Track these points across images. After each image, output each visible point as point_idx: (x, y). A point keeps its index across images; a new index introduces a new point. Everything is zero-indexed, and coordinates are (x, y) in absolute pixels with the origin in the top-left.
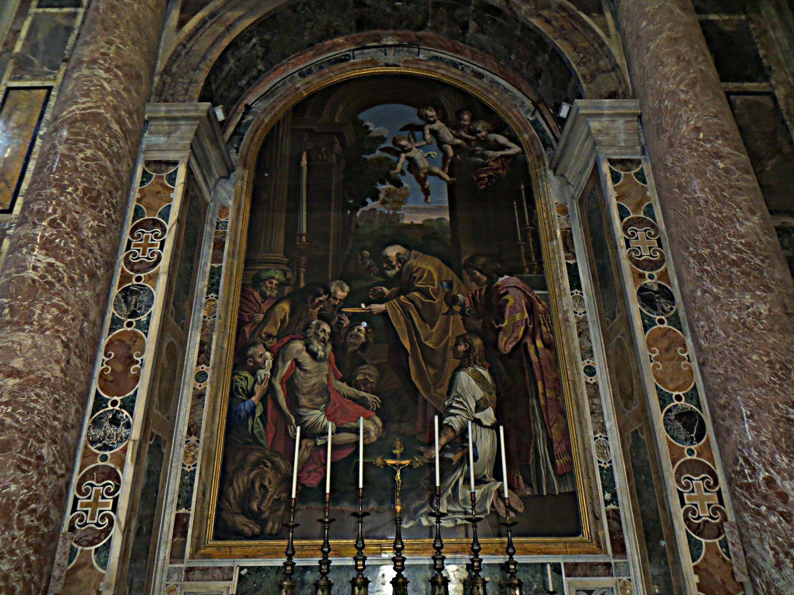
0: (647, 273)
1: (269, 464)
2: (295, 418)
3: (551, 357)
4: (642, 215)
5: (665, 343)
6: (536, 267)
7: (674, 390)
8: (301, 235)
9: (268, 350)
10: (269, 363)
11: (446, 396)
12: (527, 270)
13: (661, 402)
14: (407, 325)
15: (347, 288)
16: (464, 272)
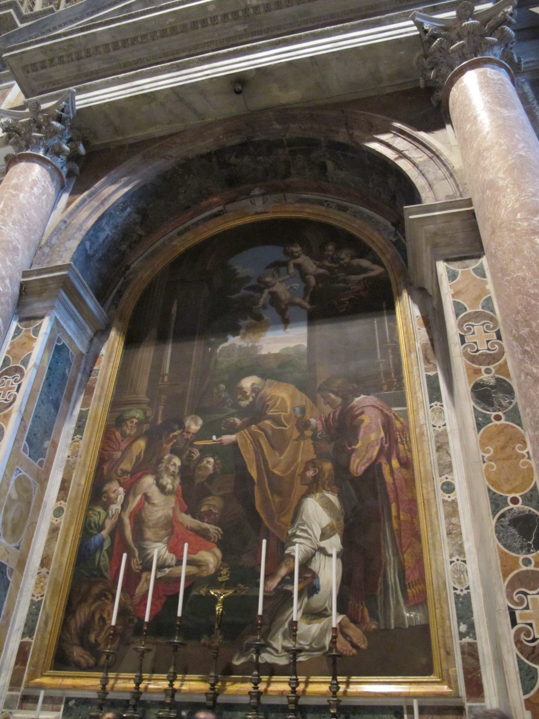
0: (483, 368)
2: (139, 551)
3: (407, 477)
4: (480, 309)
5: (502, 440)
6: (395, 383)
7: (509, 492)
8: (163, 376)
9: (121, 485)
10: (121, 498)
11: (290, 524)
12: (385, 387)
13: (494, 506)
14: (256, 453)
15: (200, 422)
16: (319, 396)
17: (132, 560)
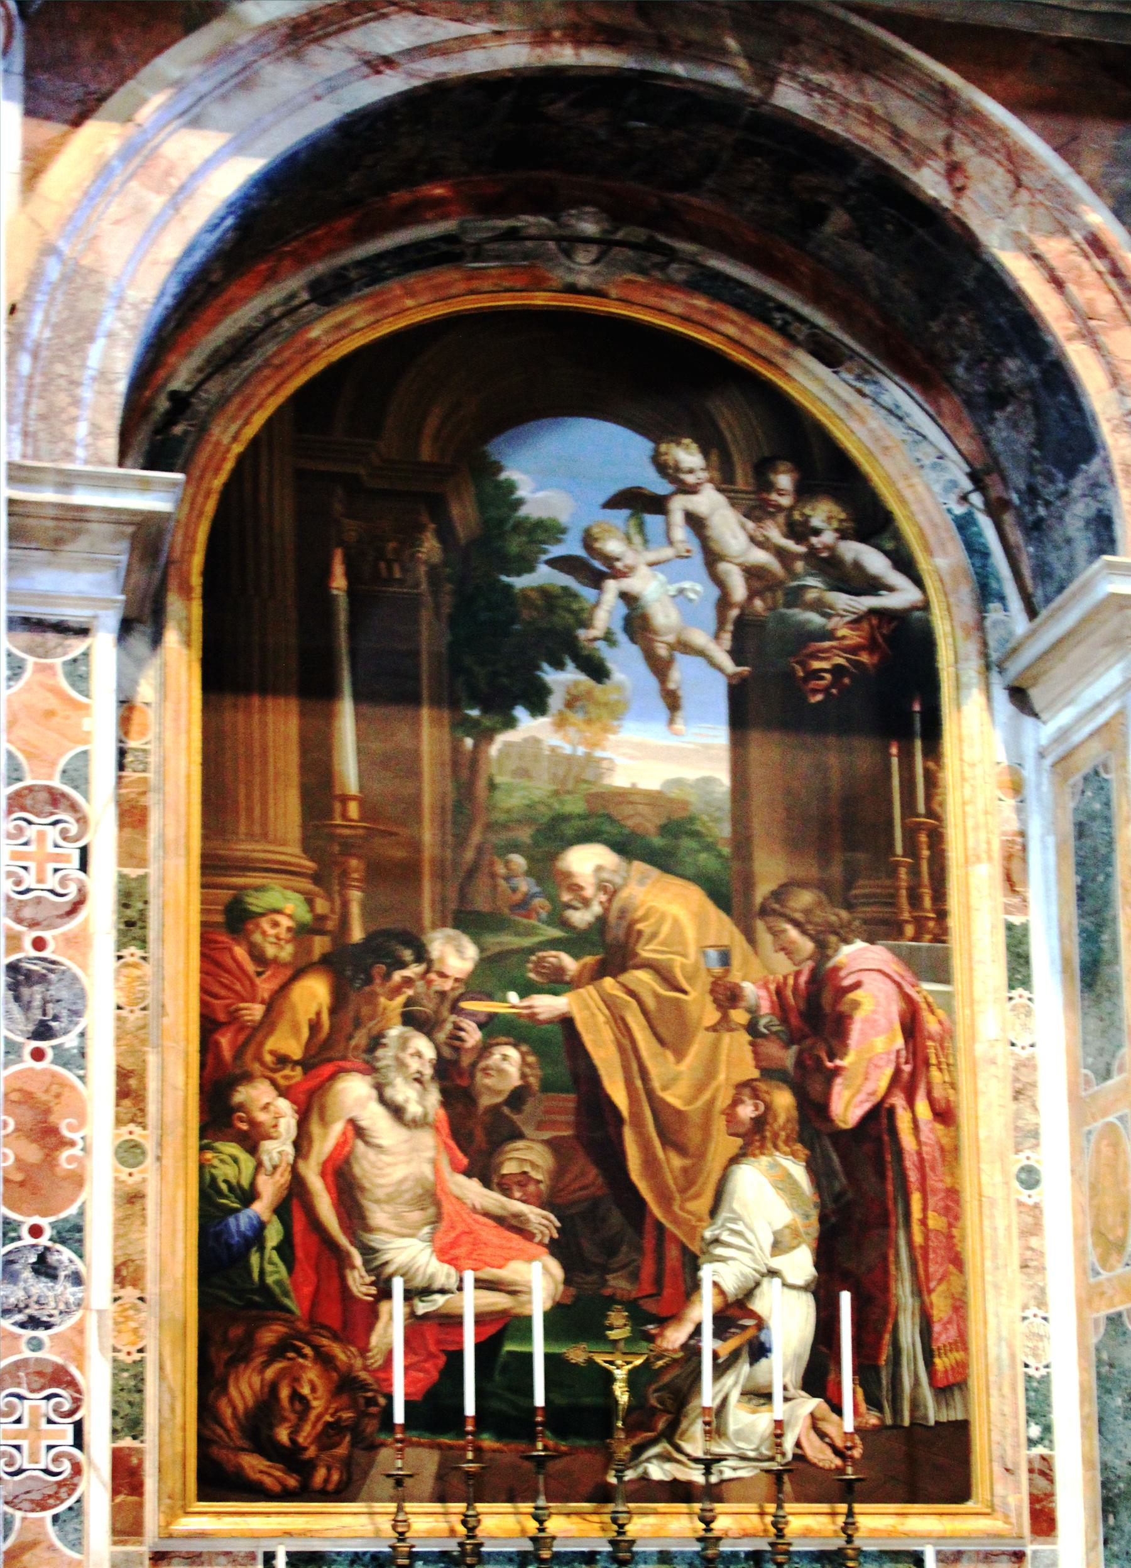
1: (308, 1350)
2: (363, 1254)
17: (348, 1272)
